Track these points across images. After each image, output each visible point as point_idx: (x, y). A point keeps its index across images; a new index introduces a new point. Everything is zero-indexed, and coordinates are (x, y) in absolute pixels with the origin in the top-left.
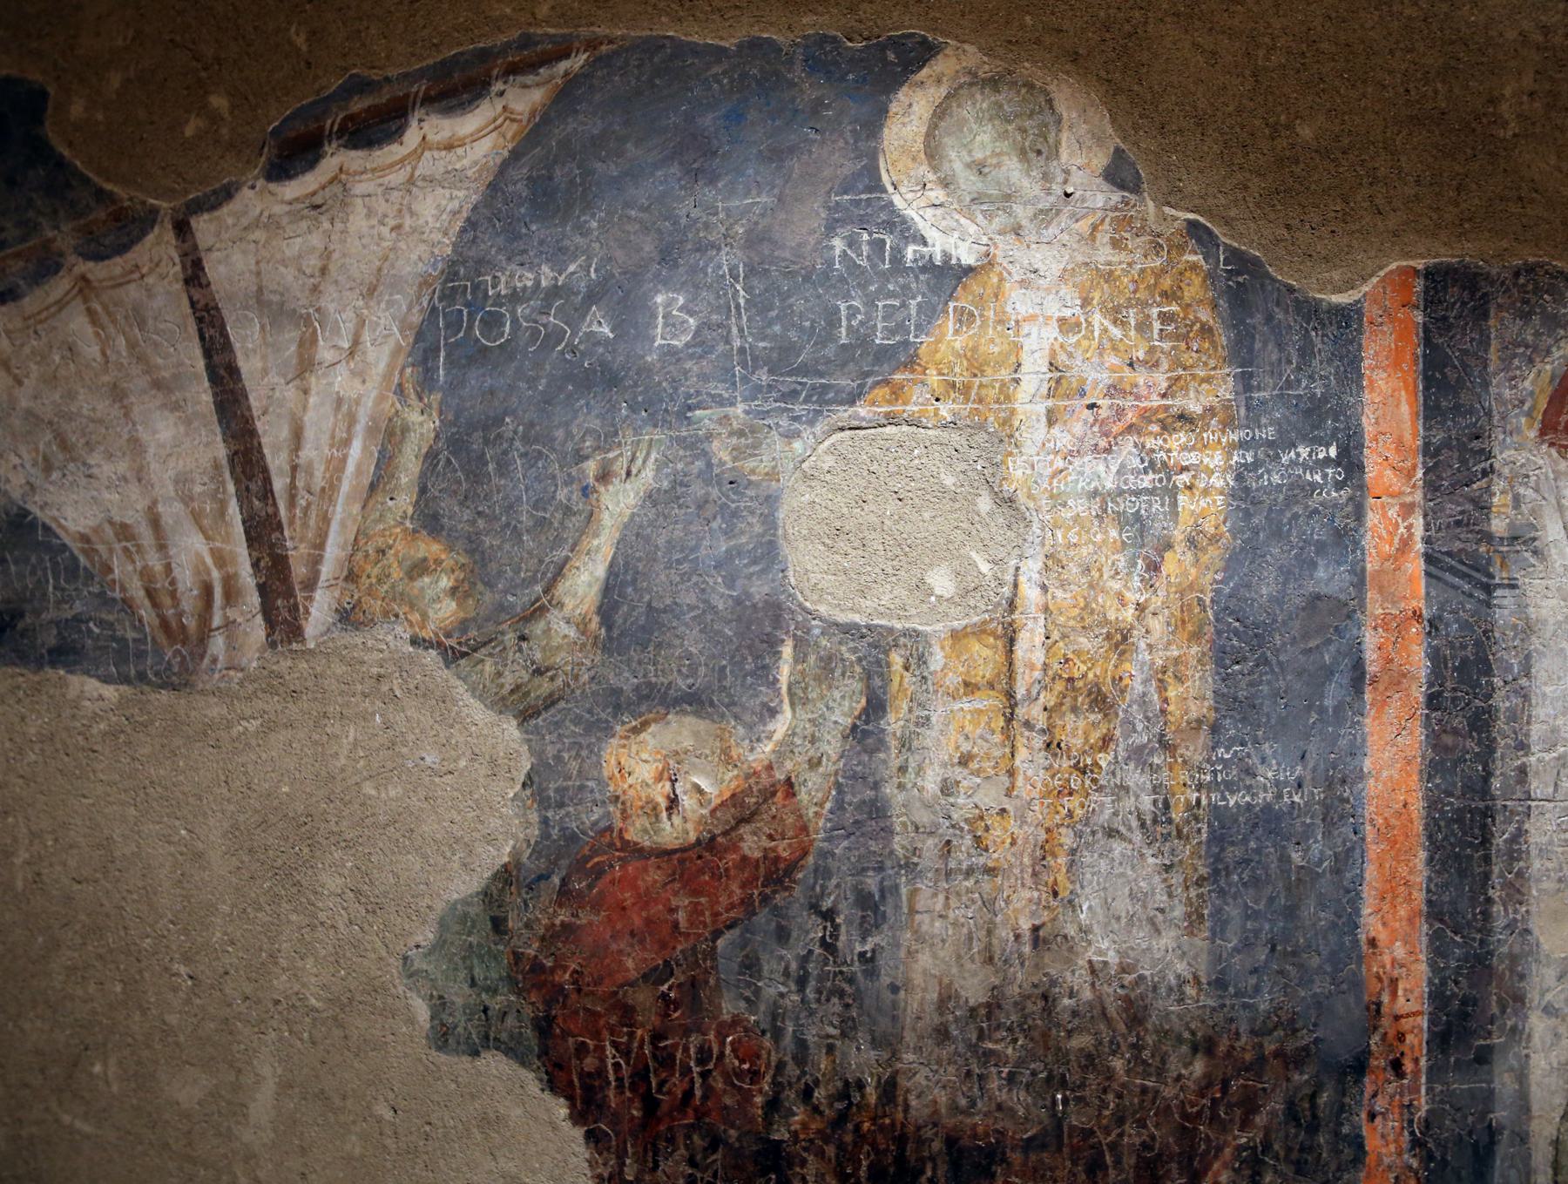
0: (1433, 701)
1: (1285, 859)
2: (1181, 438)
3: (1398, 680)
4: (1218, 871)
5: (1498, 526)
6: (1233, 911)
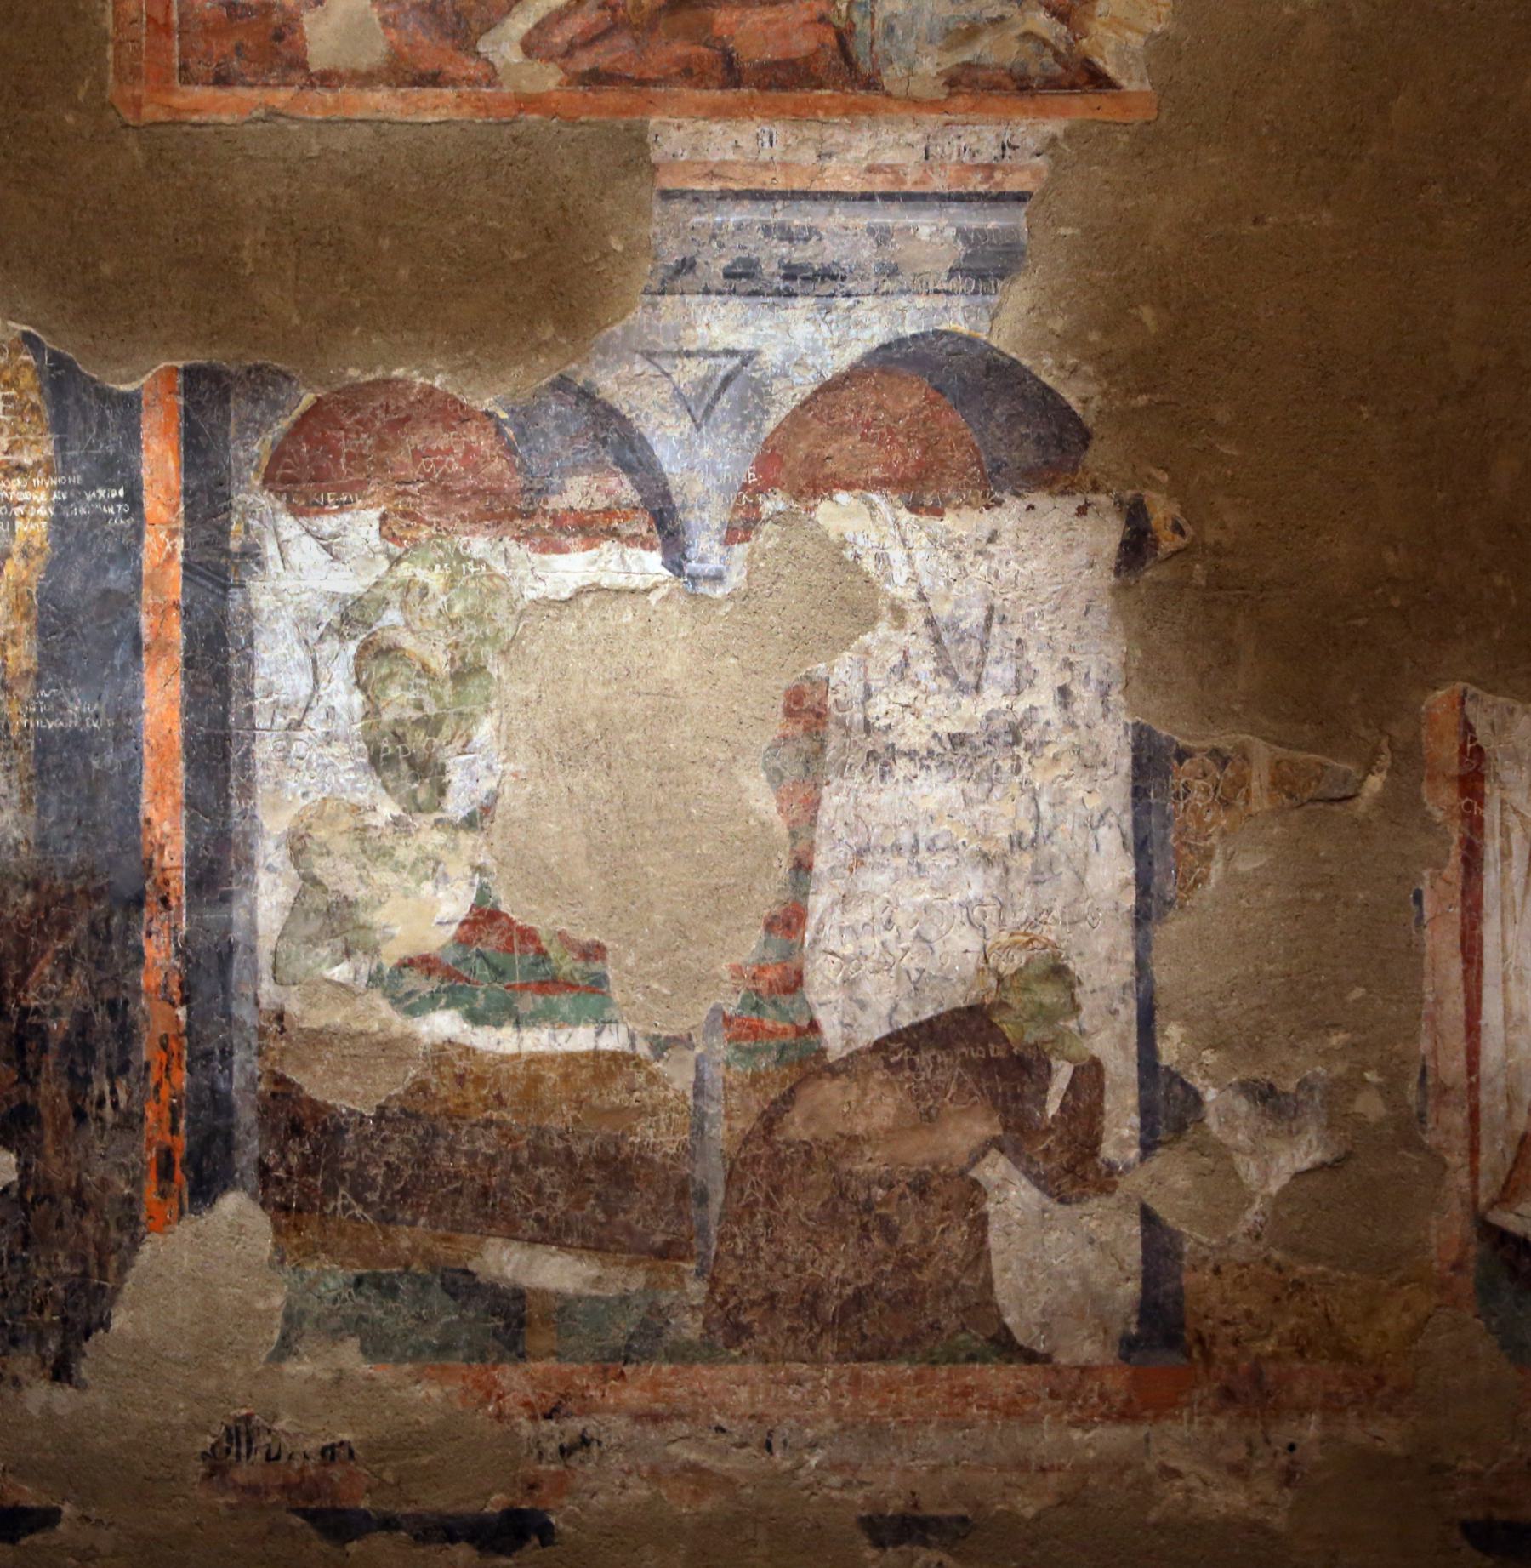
0: (188, 662)
1: (87, 765)
2: (17, 482)
3: (165, 648)
4: (42, 772)
5: (234, 545)
6: (53, 798)
